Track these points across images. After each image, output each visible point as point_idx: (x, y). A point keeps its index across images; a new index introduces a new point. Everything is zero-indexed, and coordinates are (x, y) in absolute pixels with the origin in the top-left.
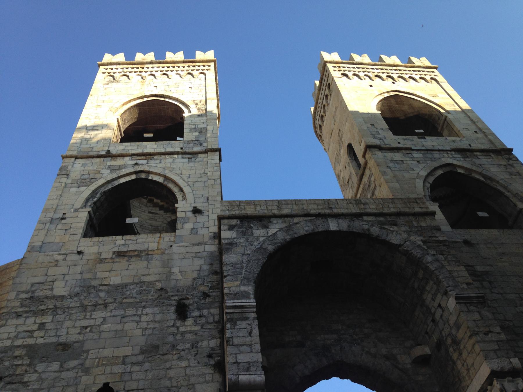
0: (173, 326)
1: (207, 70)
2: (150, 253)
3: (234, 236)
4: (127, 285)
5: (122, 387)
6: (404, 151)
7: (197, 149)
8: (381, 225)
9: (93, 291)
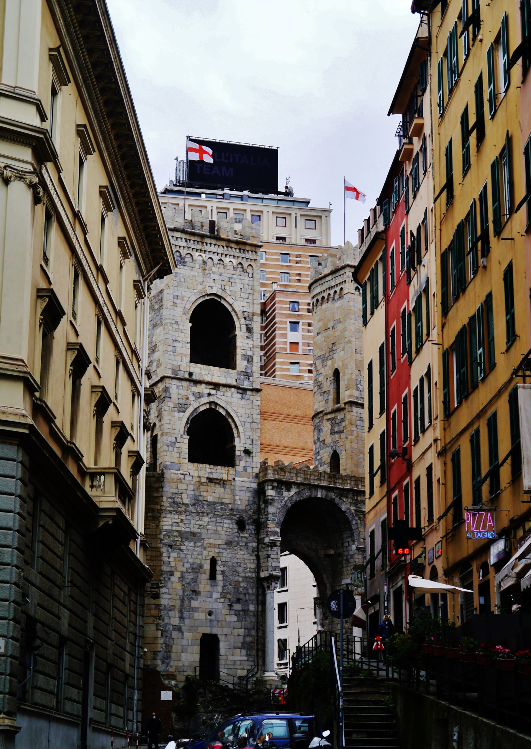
2: (225, 483)
3: (274, 495)
7: (246, 385)
9: (200, 503)
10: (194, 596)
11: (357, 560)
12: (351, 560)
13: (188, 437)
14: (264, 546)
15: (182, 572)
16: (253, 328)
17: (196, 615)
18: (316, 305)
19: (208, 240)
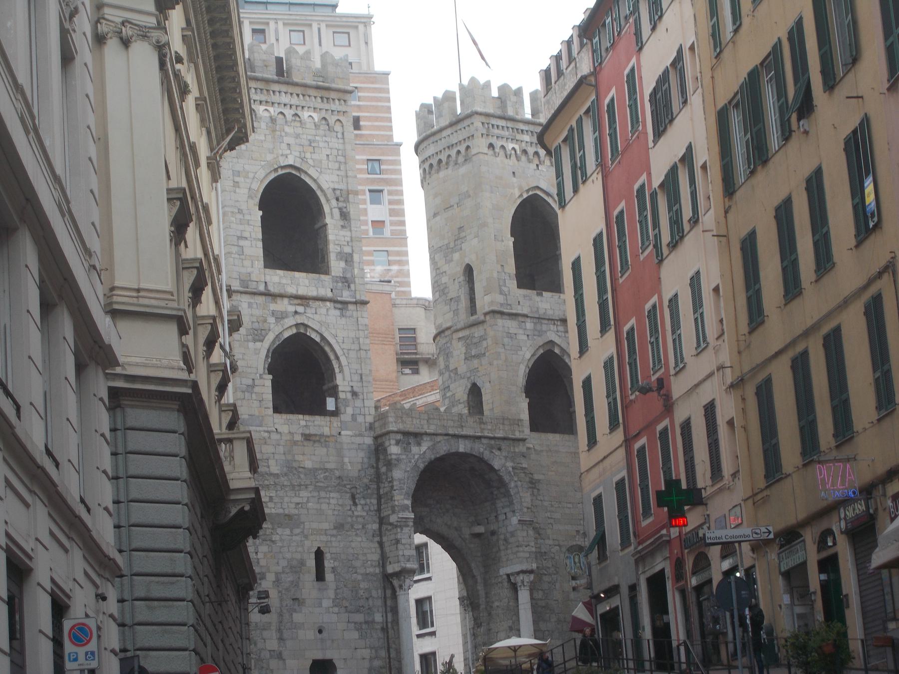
4: (317, 469)
6: (521, 319)
7: (346, 296)
8: (492, 447)
10: (296, 607)
11: (520, 539)
12: (512, 540)
13: (271, 377)
14: (389, 527)
15: (277, 574)
16: (349, 213)
17: (301, 633)
18: (430, 173)
19: (276, 87)
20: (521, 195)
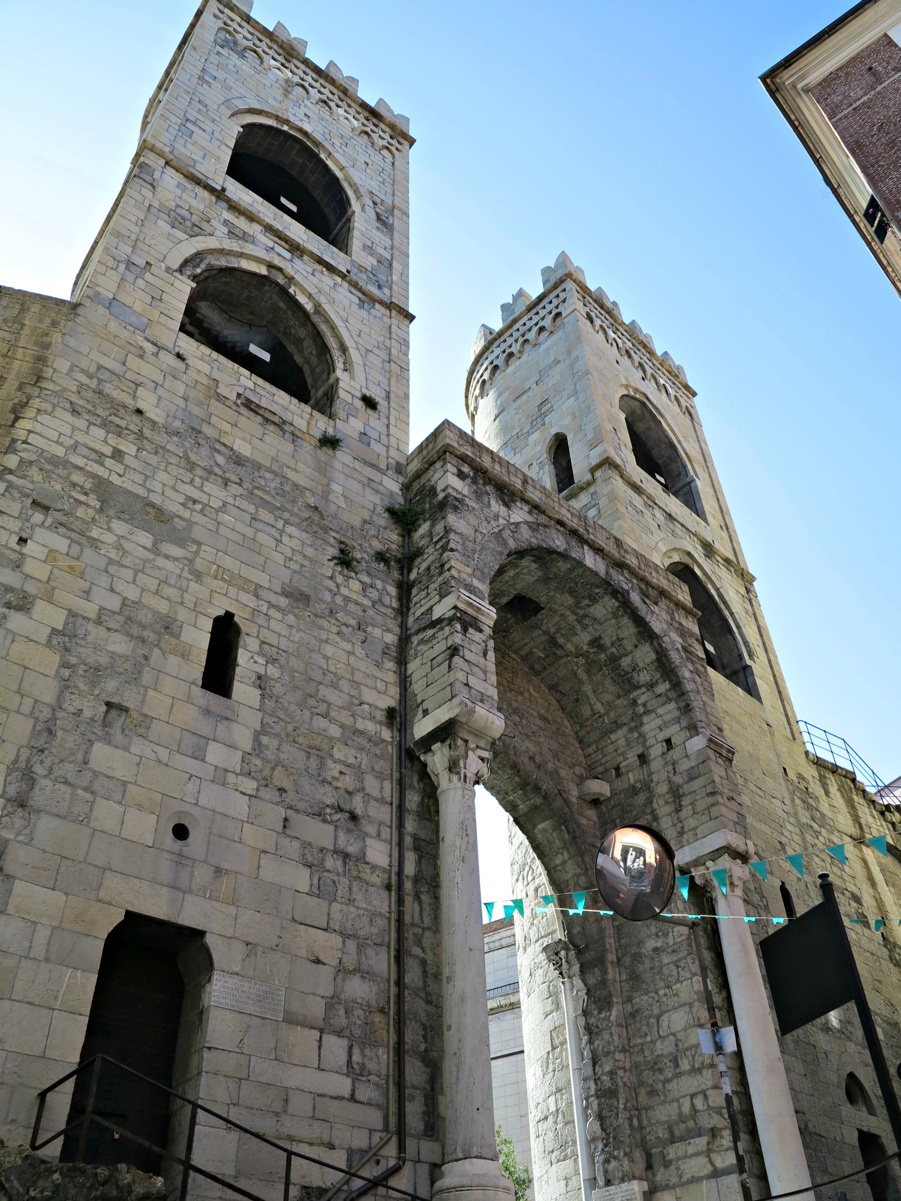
0: (331, 578)
1: (397, 149)
5: (254, 631)
7: (372, 289)
15: (72, 614)
20: (627, 387)
